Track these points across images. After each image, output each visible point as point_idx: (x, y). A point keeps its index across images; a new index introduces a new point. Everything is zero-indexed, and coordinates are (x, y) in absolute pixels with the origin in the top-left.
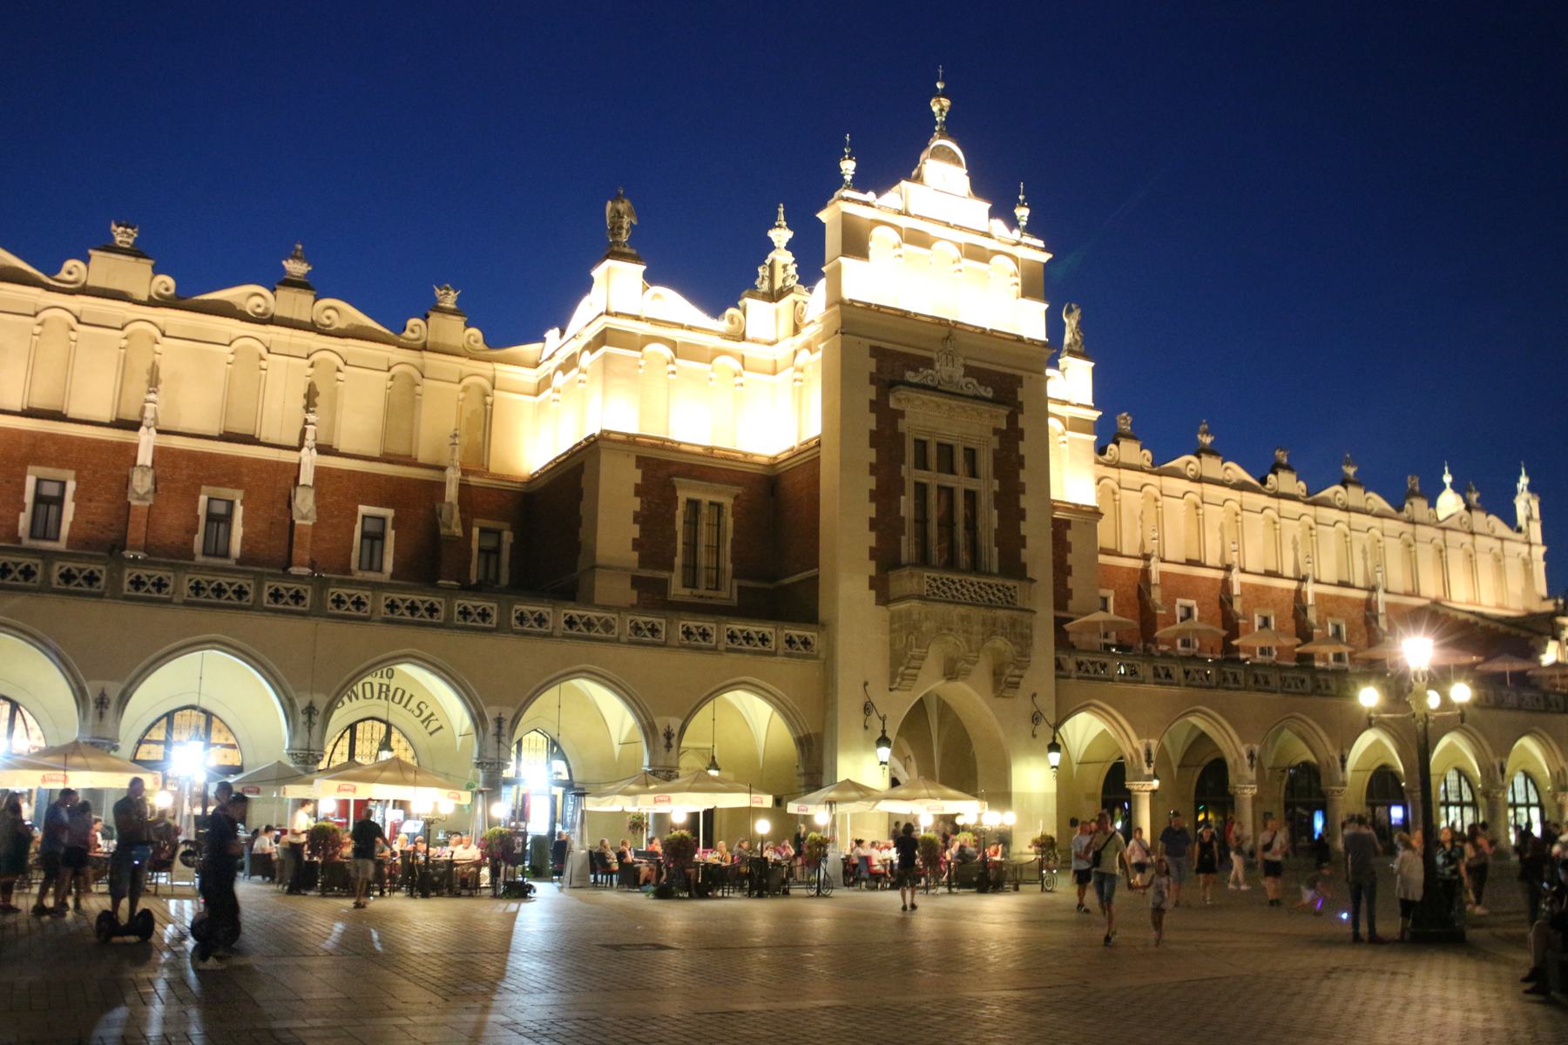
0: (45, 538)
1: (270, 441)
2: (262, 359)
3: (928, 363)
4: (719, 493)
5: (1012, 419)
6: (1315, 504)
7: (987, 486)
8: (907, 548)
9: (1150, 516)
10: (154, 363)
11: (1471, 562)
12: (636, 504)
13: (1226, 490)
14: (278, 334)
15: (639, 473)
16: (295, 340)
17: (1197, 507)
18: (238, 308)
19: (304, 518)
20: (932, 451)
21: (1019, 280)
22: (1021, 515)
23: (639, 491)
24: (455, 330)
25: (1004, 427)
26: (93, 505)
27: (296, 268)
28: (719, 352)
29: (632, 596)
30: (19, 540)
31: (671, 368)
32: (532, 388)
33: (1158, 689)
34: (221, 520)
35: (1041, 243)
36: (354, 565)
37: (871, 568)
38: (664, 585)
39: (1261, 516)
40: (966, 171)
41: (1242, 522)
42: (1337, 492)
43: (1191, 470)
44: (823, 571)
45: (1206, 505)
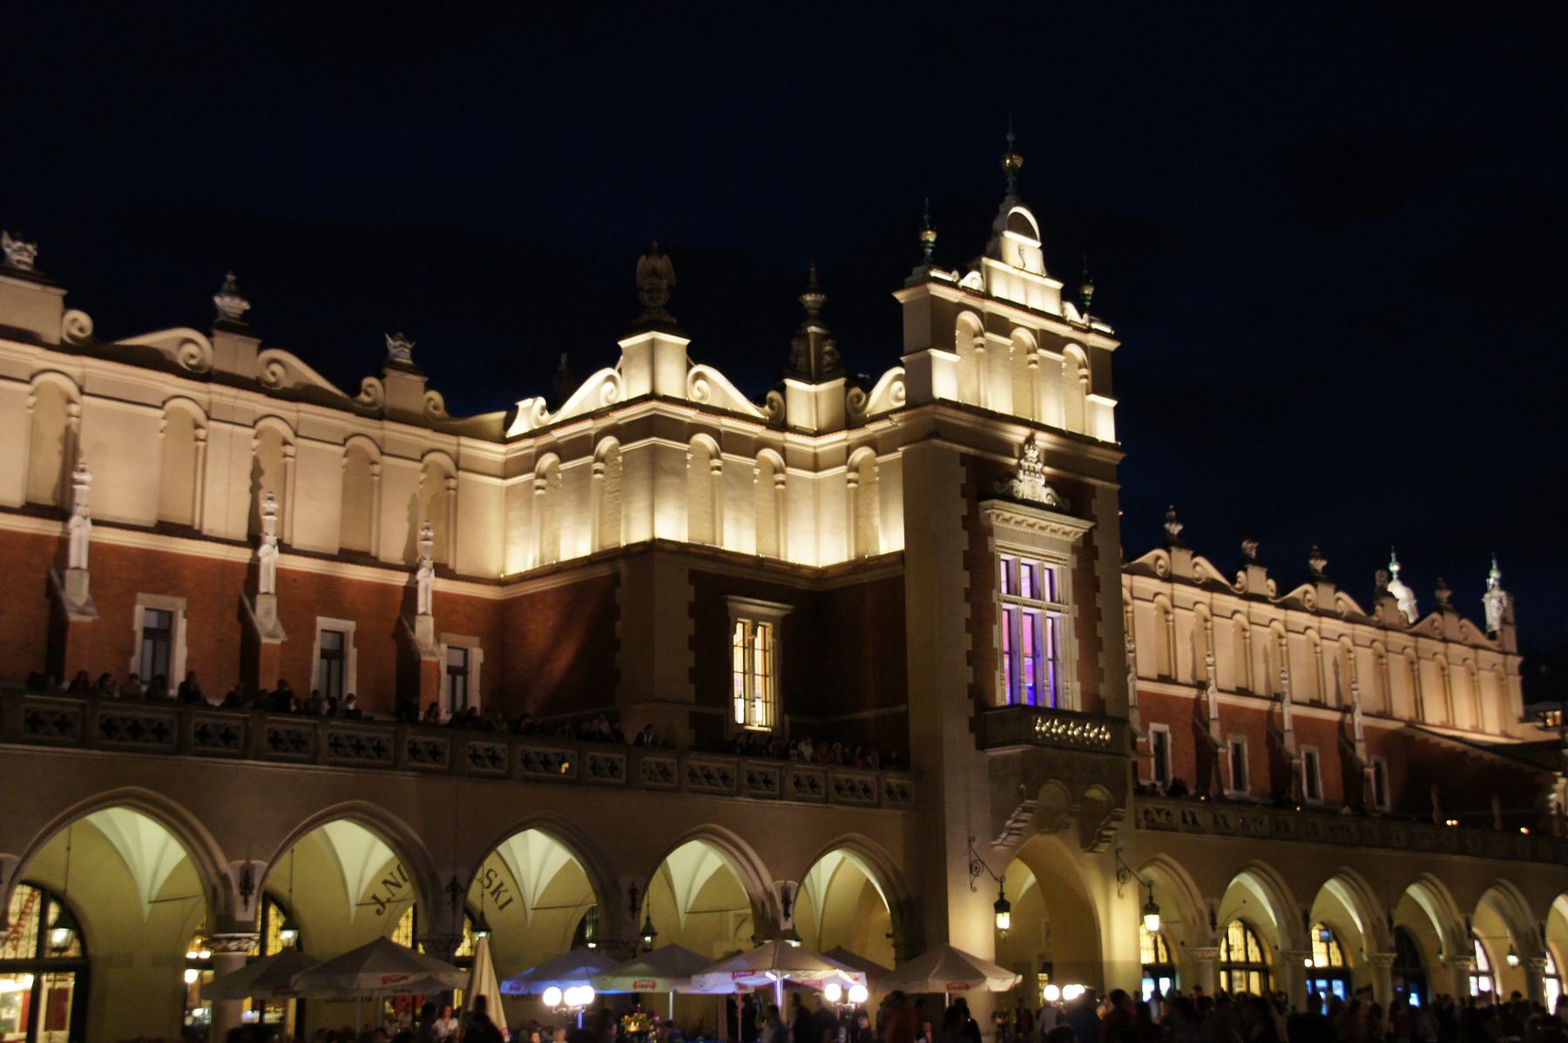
1: (215, 535)
2: (286, 443)
6: (1285, 606)
10: (68, 428)
11: (1443, 676)
13: (1196, 591)
14: (221, 394)
15: (692, 588)
16: (239, 403)
18: (168, 358)
19: (272, 635)
28: (763, 444)
31: (716, 462)
35: (1107, 330)
39: (1230, 622)
40: (1039, 244)
41: (1212, 629)
42: (1306, 592)
43: (1161, 567)
45: (1177, 611)
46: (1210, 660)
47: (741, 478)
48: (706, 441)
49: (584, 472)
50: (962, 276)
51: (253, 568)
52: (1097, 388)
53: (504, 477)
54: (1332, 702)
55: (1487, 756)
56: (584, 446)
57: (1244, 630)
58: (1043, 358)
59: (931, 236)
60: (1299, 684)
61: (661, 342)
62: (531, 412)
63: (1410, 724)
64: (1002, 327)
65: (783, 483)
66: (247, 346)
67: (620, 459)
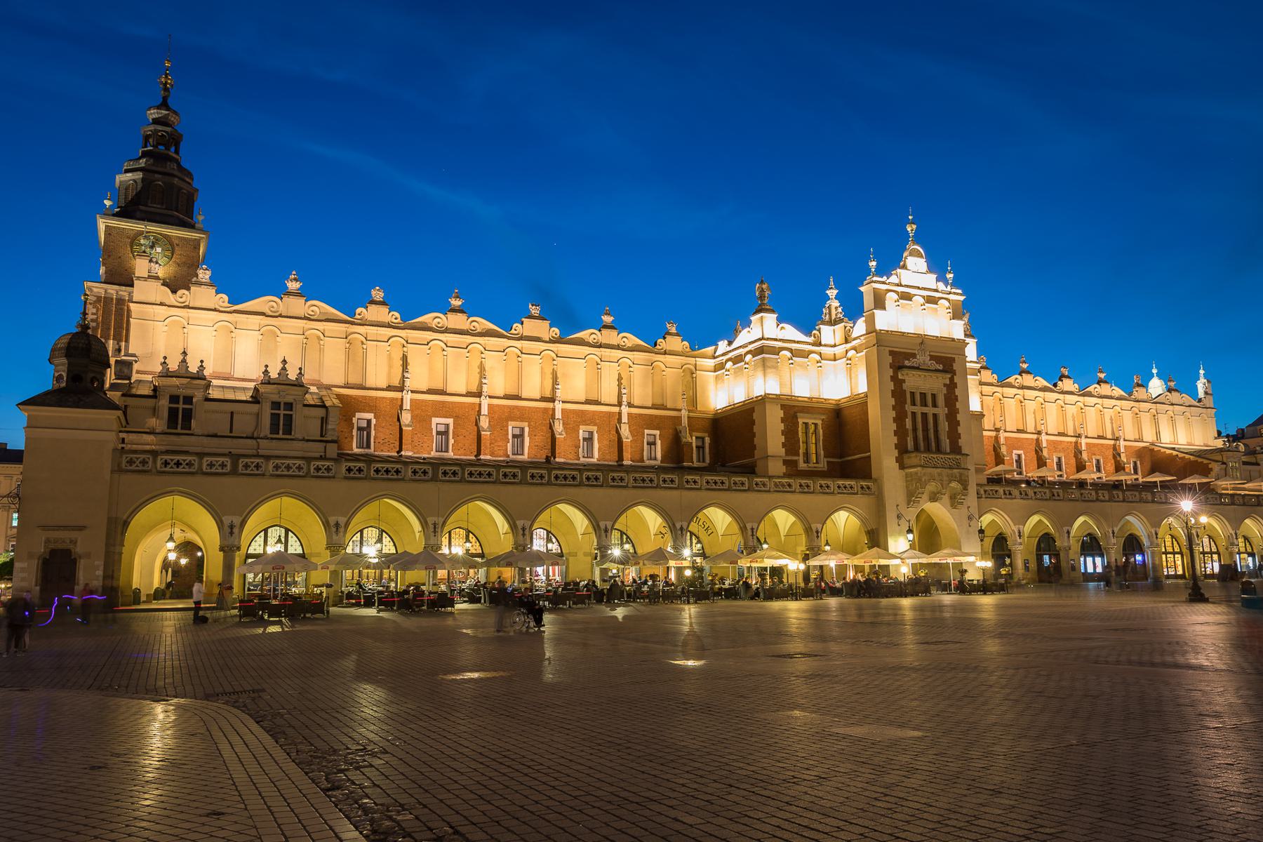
0: (517, 454)
3: (914, 356)
4: (815, 419)
5: (952, 379)
7: (942, 411)
8: (910, 444)
9: (998, 408)
12: (782, 426)
16: (612, 354)
17: (1021, 402)
20: (918, 397)
21: (951, 311)
22: (958, 423)
23: (783, 420)
24: (675, 343)
25: (948, 383)
26: (536, 438)
27: (608, 319)
29: (783, 469)
30: (508, 456)
31: (791, 361)
32: (712, 369)
33: (1022, 501)
34: (589, 440)
35: (960, 291)
36: (645, 458)
37: (896, 453)
38: (795, 463)
40: (925, 260)
44: (873, 453)
46: (1042, 422)
47: (805, 367)
48: (788, 354)
49: (740, 369)
50: (888, 279)
51: (620, 414)
52: (956, 316)
53: (715, 372)
54: (1109, 436)
55: (1187, 456)
56: (738, 359)
57: (1062, 407)
58: (928, 308)
59: (874, 263)
60: (1092, 430)
61: (765, 317)
62: (723, 346)
63: (1152, 444)
64: (907, 297)
65: (821, 367)
66: (614, 333)
67: (753, 363)
